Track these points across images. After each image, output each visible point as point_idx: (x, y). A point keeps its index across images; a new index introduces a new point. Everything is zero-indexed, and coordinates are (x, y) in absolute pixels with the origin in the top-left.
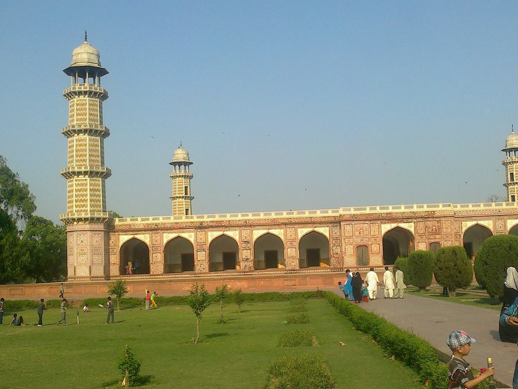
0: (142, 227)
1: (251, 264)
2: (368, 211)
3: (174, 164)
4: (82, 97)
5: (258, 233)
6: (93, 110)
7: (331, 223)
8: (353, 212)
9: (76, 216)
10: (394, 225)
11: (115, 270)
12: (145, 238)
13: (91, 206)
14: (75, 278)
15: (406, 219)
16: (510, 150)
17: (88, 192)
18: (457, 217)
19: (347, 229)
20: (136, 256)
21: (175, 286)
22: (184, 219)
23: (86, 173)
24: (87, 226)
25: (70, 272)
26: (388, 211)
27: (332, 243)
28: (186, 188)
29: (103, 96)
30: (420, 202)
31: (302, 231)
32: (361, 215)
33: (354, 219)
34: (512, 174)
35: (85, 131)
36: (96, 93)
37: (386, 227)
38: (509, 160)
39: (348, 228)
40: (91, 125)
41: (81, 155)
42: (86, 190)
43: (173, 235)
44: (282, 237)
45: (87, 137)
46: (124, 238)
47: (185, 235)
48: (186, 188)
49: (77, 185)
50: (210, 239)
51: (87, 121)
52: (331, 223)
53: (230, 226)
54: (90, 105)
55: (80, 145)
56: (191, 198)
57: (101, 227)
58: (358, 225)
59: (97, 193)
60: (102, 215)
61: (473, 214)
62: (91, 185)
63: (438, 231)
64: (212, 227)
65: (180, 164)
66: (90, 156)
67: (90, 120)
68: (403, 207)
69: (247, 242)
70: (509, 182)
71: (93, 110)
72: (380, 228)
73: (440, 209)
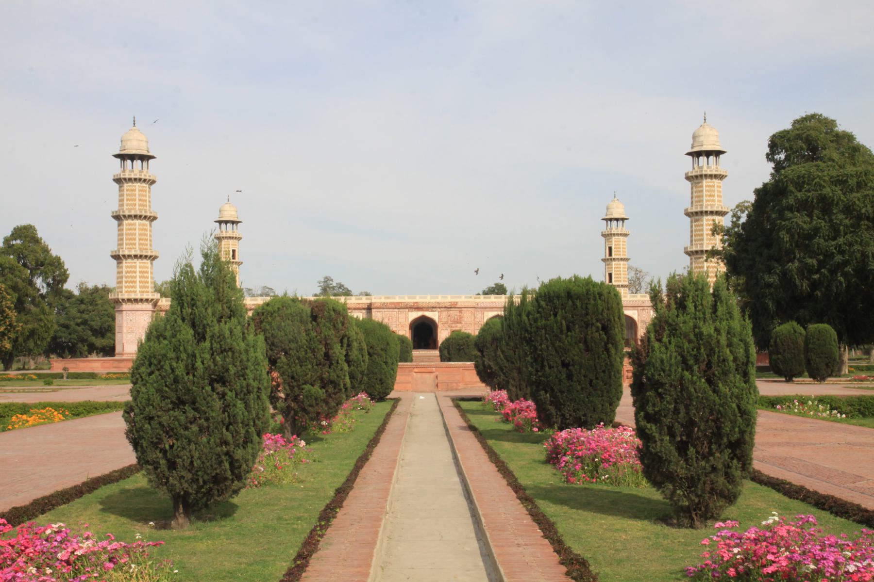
2: (397, 300)
4: (130, 184)
6: (143, 195)
8: (383, 300)
9: (126, 297)
10: (419, 314)
13: (140, 287)
14: (122, 354)
15: (432, 308)
16: (611, 220)
17: (138, 274)
23: (136, 256)
25: (118, 349)
26: (415, 301)
28: (234, 251)
32: (391, 303)
34: (610, 249)
36: (145, 180)
37: (414, 315)
40: (141, 211)
41: (131, 239)
42: (135, 272)
48: (234, 251)
51: (137, 207)
54: (140, 191)
55: (130, 229)
56: (239, 264)
57: (149, 306)
59: (146, 275)
60: (150, 297)
61: (494, 305)
62: (140, 267)
66: (140, 239)
67: (140, 205)
68: (429, 297)
70: (608, 257)
71: (143, 195)
72: (407, 315)
73: (462, 300)
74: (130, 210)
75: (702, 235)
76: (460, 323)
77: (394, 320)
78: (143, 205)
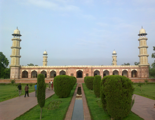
0: (27, 68)
1: (49, 77)
3: (44, 54)
4: (15, 40)
5: (51, 70)
7: (66, 69)
9: (12, 65)
11: (21, 77)
12: (27, 70)
13: (16, 63)
16: (114, 54)
17: (15, 61)
18: (92, 69)
19: (69, 70)
20: (25, 74)
21: (31, 81)
22: (45, 67)
23: (15, 56)
24: (15, 68)
25: (11, 77)
27: (66, 73)
29: (20, 40)
30: (85, 65)
31: (60, 70)
33: (71, 68)
35: (15, 48)
37: (77, 70)
38: (113, 56)
39: (69, 70)
43: (33, 70)
44: (56, 71)
45: (16, 49)
46: (23, 70)
47: (36, 70)
49: (13, 59)
50: (41, 71)
52: (66, 69)
53: (45, 68)
56: (47, 62)
57: (18, 68)
58: (71, 69)
60: (18, 65)
63: (88, 71)
64: (41, 69)
65: (45, 54)
69: (48, 72)
73: (89, 66)
74: (14, 46)
75: (143, 52)
76: (88, 72)
77: (73, 71)
78: (18, 45)
